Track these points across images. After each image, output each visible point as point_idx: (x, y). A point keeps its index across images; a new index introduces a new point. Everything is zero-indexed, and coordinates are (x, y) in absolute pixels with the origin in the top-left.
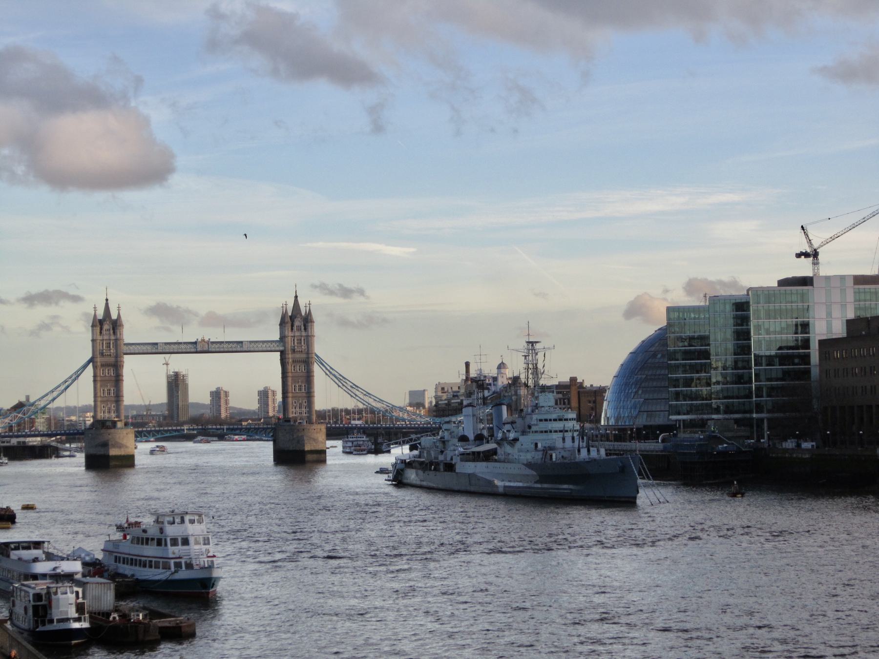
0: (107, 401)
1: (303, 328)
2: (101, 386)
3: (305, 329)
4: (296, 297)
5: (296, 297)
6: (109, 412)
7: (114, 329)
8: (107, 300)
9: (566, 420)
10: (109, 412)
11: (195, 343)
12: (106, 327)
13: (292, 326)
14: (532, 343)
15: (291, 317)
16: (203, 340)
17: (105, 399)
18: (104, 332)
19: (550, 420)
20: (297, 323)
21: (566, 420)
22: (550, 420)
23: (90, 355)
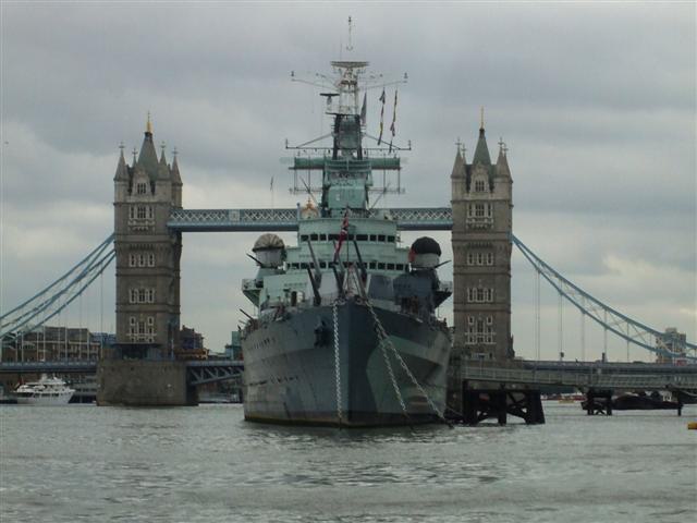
0: (139, 312)
1: (487, 185)
3: (492, 188)
4: (482, 131)
5: (482, 131)
6: (142, 331)
7: (152, 184)
8: (148, 135)
9: (363, 238)
10: (142, 331)
11: (294, 212)
12: (142, 180)
13: (468, 182)
14: (351, 65)
15: (468, 169)
16: (309, 206)
17: (136, 308)
18: (135, 190)
19: (323, 237)
20: (479, 176)
21: (363, 238)
22: (323, 237)
23: (111, 230)
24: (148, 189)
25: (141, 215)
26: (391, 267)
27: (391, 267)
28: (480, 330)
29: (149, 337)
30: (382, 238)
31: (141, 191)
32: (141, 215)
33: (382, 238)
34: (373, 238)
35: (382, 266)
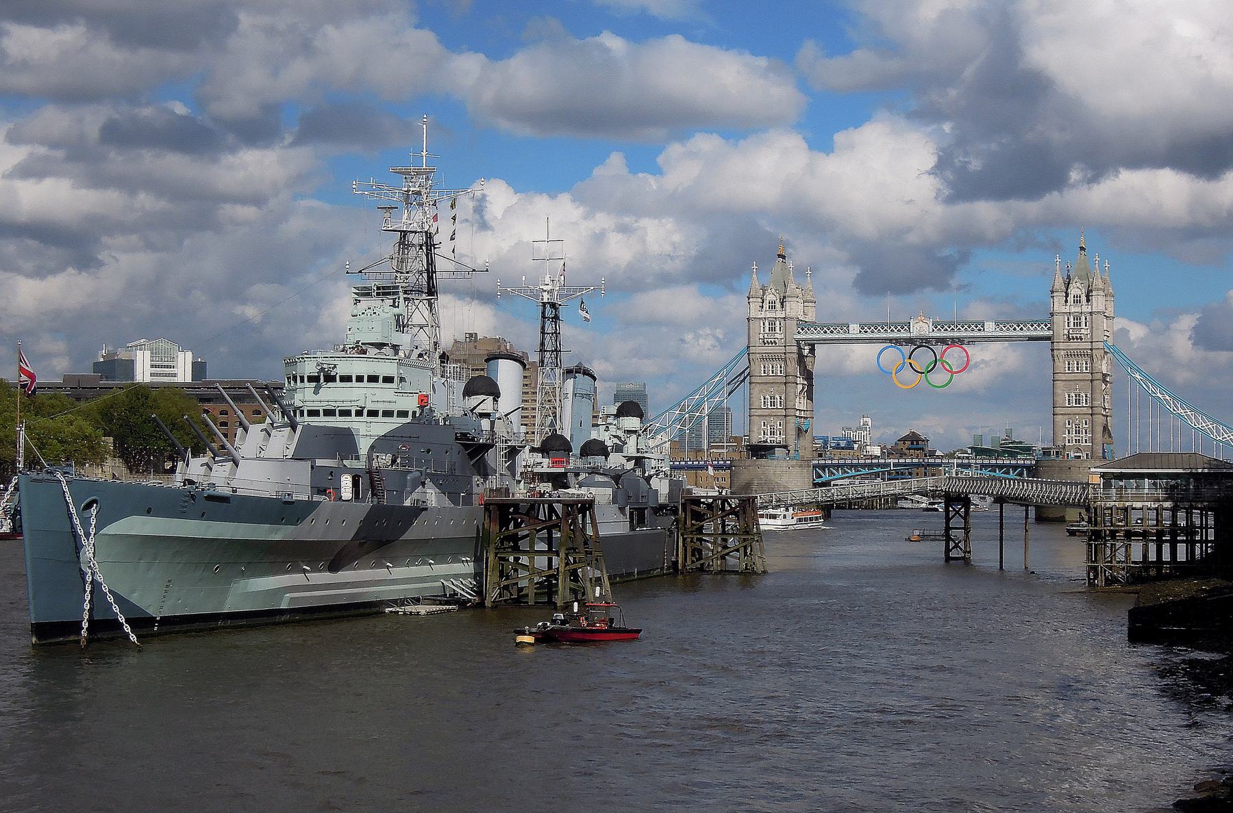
1: (1084, 298)
2: (761, 391)
6: (772, 433)
9: (346, 379)
10: (772, 433)
17: (766, 412)
18: (766, 305)
21: (346, 379)
24: (778, 305)
25: (772, 329)
26: (387, 414)
27: (387, 414)
28: (1077, 432)
29: (778, 438)
30: (373, 379)
31: (772, 307)
32: (772, 329)
33: (373, 379)
34: (360, 379)
35: (373, 413)
